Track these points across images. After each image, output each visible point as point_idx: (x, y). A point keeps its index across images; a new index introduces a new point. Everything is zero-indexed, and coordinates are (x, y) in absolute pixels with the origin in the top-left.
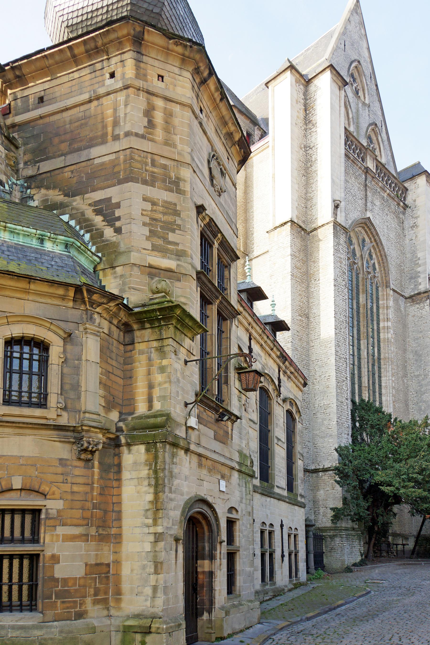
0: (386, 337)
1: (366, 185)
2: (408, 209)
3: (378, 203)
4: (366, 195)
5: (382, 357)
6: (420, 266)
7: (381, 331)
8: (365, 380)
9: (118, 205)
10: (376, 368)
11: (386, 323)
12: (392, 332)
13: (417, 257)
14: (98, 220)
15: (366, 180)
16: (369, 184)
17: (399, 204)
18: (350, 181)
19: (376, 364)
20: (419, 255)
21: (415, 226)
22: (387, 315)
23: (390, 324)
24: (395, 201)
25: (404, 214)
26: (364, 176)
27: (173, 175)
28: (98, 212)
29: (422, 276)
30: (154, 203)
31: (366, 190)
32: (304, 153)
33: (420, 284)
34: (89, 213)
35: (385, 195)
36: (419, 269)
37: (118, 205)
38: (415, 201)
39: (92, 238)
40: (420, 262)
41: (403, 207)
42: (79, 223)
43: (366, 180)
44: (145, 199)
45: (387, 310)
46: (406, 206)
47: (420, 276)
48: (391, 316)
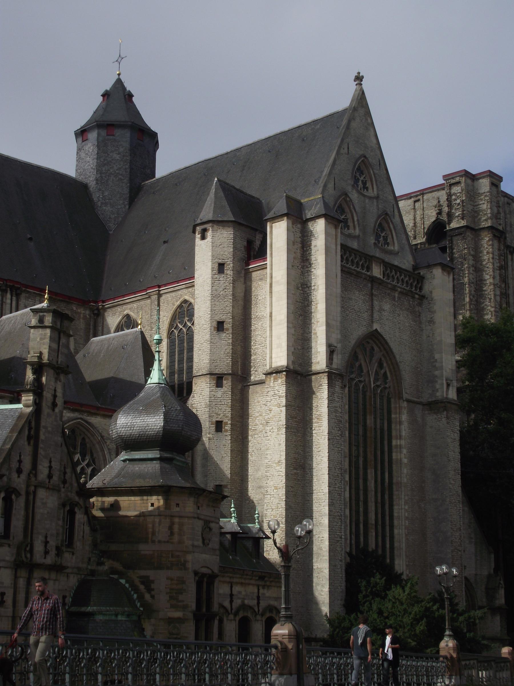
0: (399, 457)
1: (372, 295)
2: (425, 301)
3: (387, 307)
4: (372, 305)
5: (394, 481)
6: (437, 370)
7: (394, 450)
8: (372, 516)
9: (153, 582)
10: (386, 497)
11: (399, 441)
12: (405, 451)
13: (434, 358)
14: (142, 587)
15: (372, 289)
16: (375, 292)
17: (413, 297)
18: (353, 297)
19: (387, 492)
20: (437, 356)
21: (431, 322)
22: (400, 432)
23: (403, 442)
24: (409, 296)
25: (420, 305)
26: (370, 285)
27: (182, 560)
28: (143, 583)
29: (439, 382)
30: (172, 579)
31: (372, 300)
32: (302, 292)
33: (437, 390)
34: (137, 582)
35: (397, 295)
36: (437, 373)
37: (153, 582)
38: (431, 292)
39: (138, 597)
40: (438, 365)
41: (418, 299)
42: (131, 586)
43: (372, 289)
44: (167, 579)
45: (400, 425)
46: (423, 297)
47: (436, 382)
48: (403, 433)
